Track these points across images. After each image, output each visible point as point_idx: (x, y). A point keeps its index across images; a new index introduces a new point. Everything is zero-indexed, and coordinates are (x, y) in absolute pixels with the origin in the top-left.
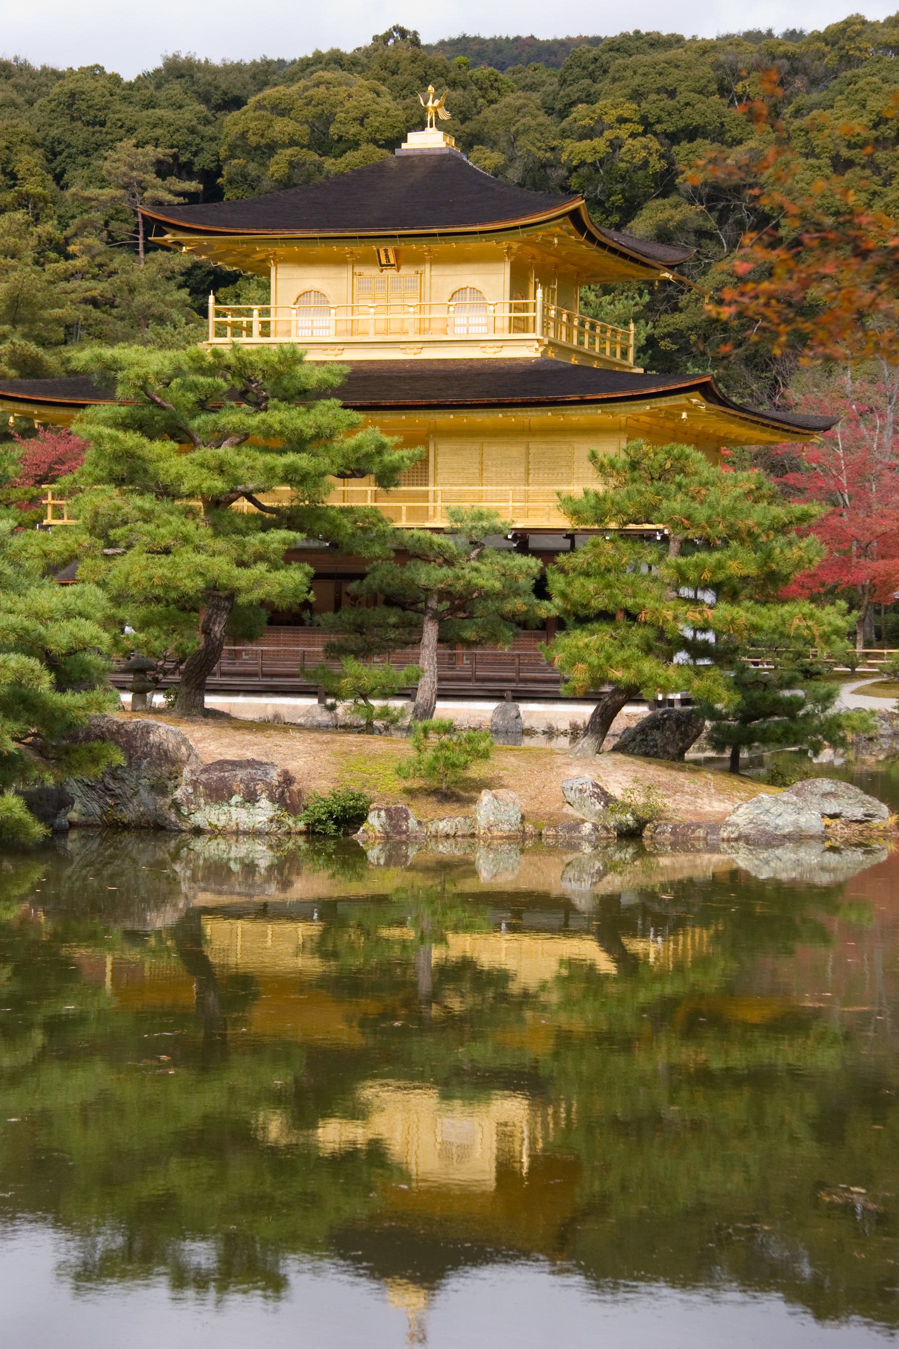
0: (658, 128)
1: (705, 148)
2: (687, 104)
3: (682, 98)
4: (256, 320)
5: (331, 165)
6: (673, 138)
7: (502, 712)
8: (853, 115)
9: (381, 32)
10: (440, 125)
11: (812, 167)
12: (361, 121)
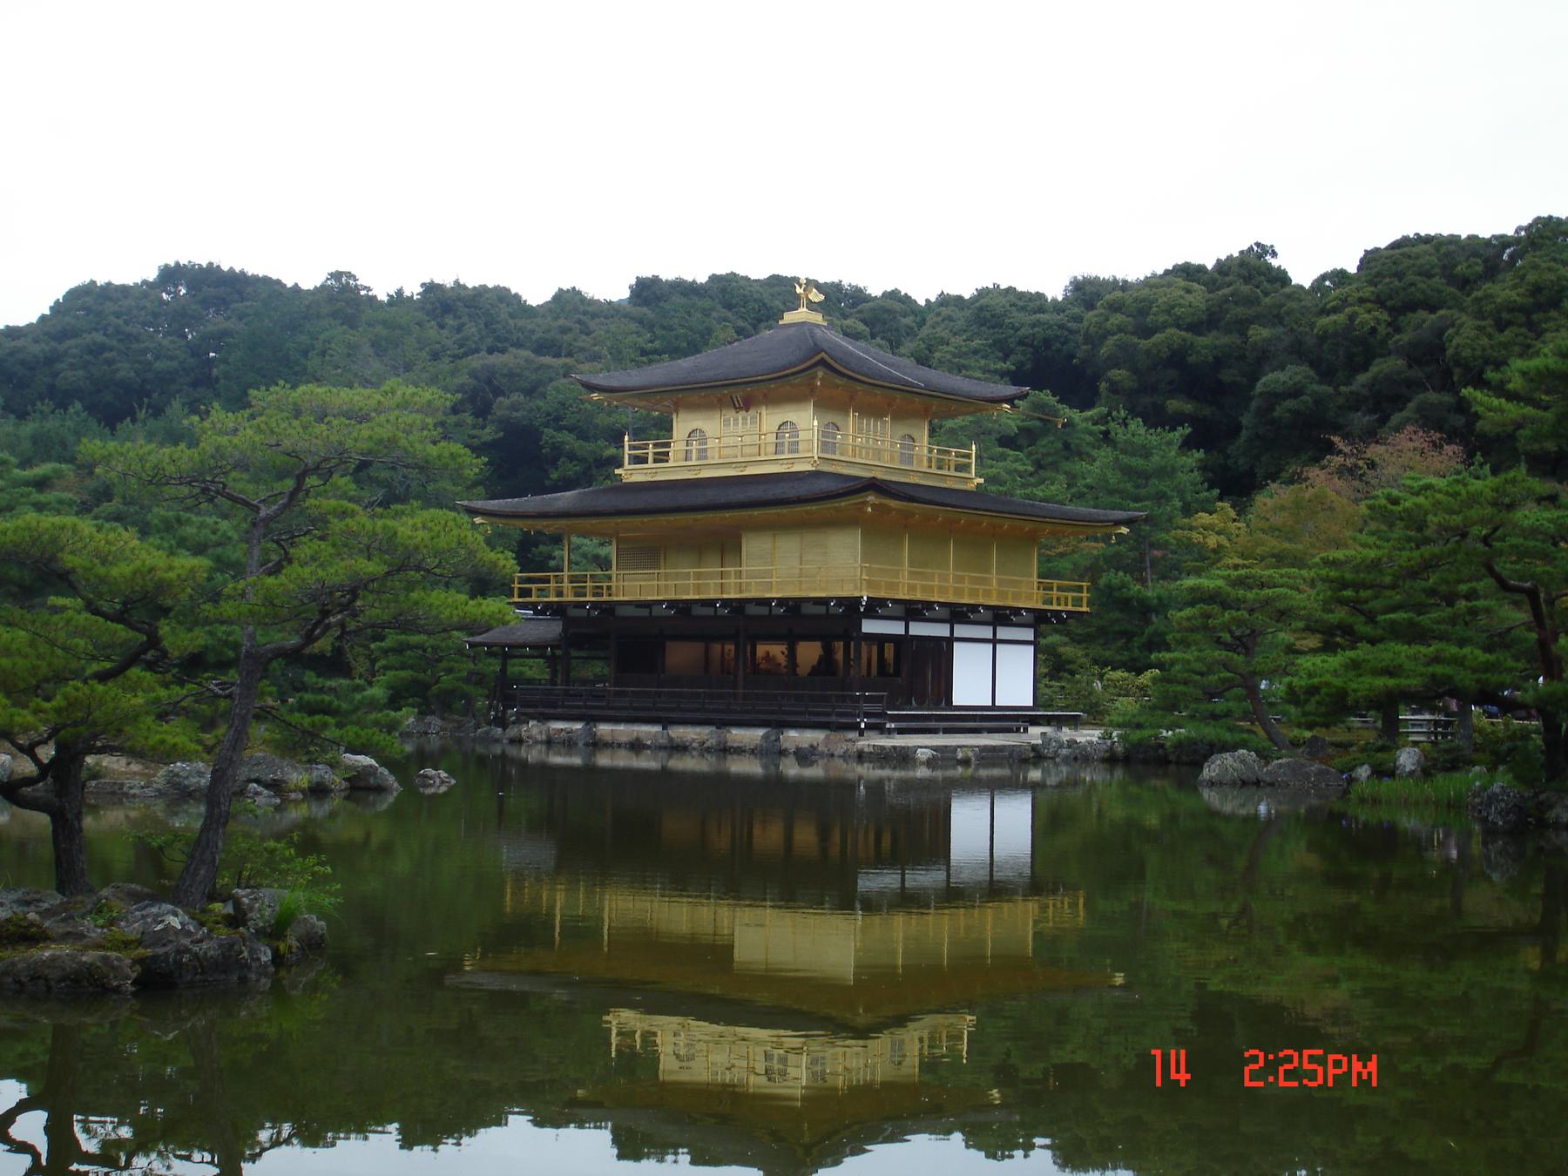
0: (1389, 303)
1: (1422, 314)
2: (1412, 284)
3: (1410, 278)
4: (651, 450)
5: (1144, 344)
6: (1411, 306)
7: (765, 737)
8: (1515, 287)
9: (1245, 248)
10: (811, 306)
11: (1479, 328)
12: (1168, 312)
